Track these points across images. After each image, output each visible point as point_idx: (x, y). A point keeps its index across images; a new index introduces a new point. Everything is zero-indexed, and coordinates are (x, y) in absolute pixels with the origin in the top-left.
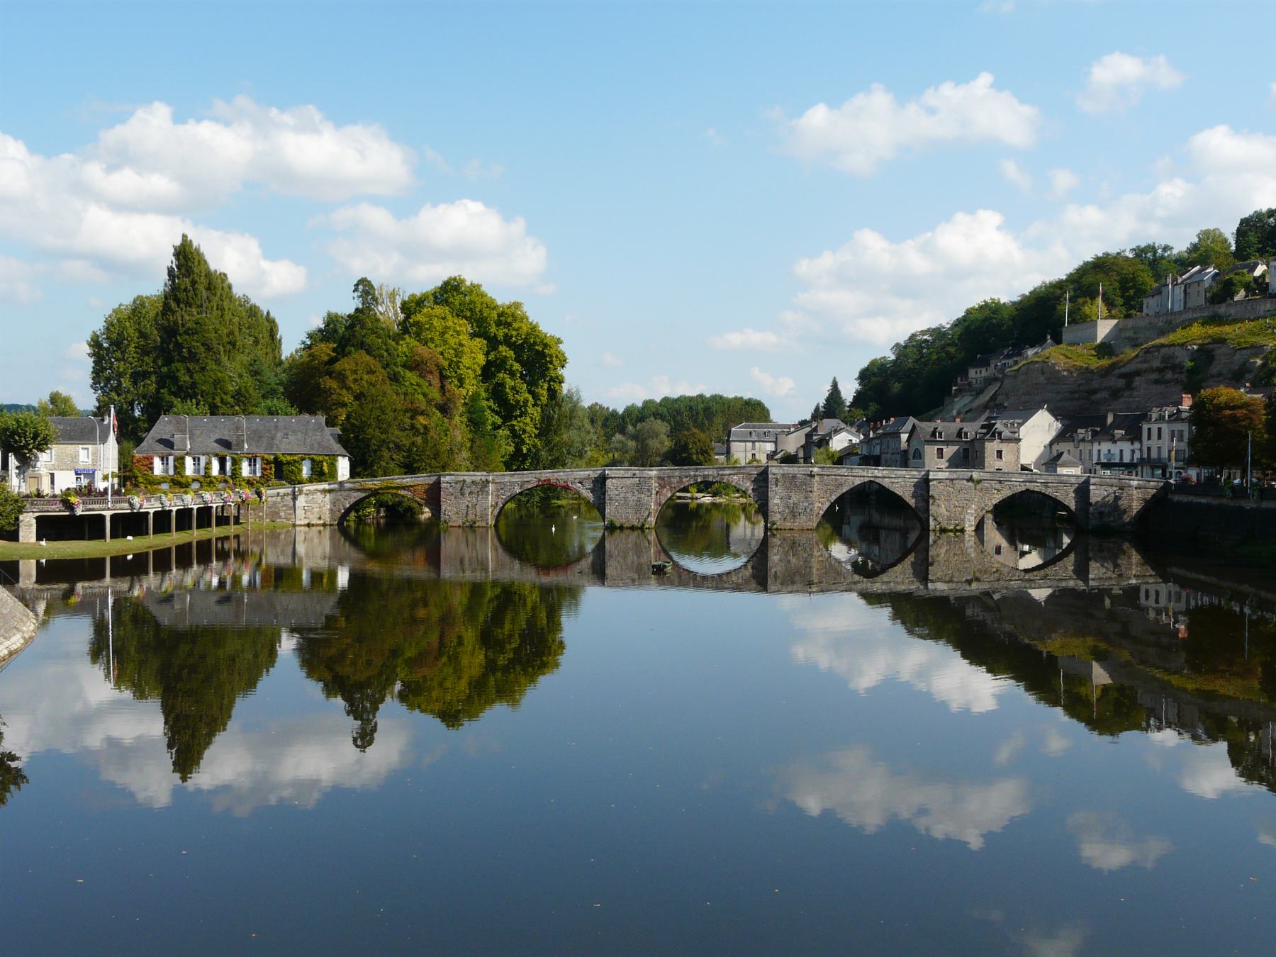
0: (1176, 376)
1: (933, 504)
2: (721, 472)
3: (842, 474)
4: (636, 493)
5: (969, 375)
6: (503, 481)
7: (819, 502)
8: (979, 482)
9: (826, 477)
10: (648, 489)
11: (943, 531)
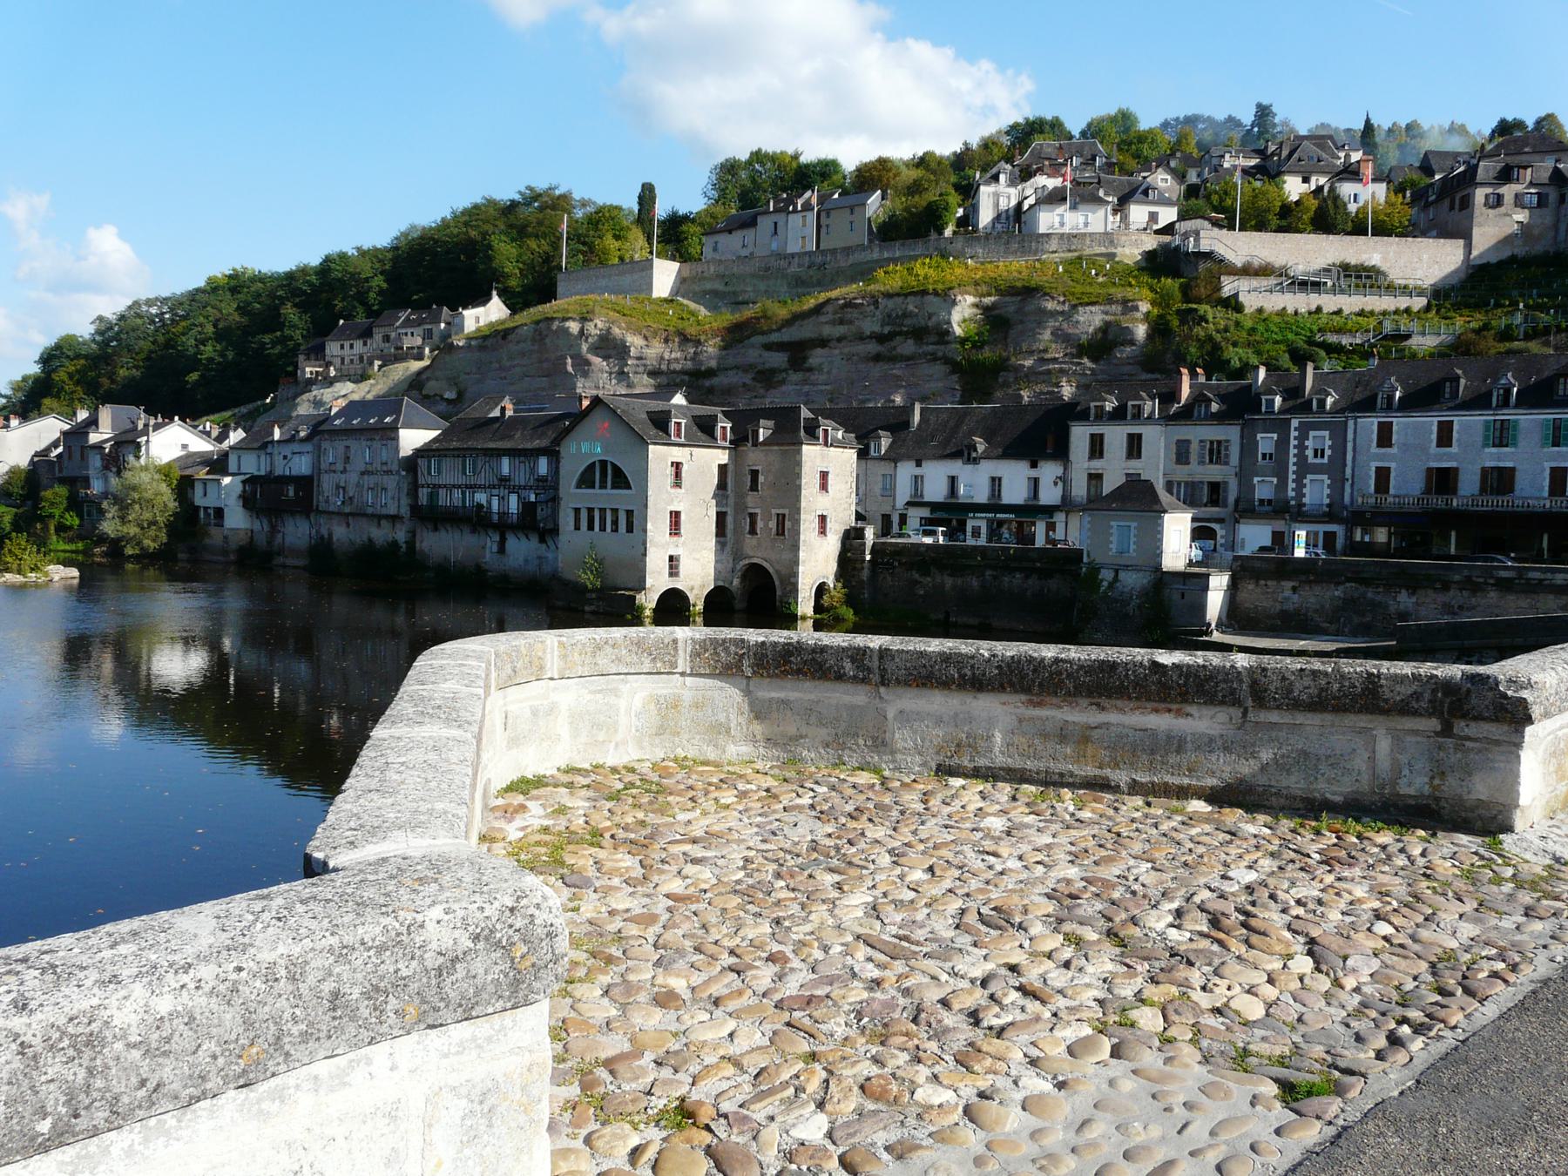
0: (931, 348)
5: (328, 351)
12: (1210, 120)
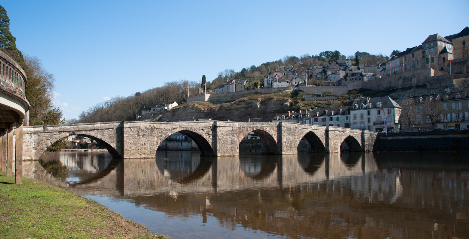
2: (263, 125)
3: (303, 128)
4: (231, 136)
6: (161, 127)
10: (236, 133)
12: (331, 52)
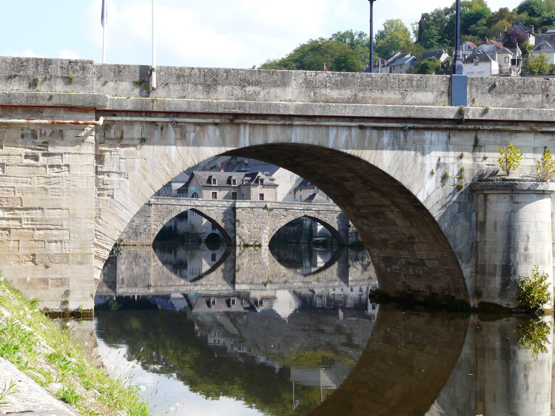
1: (238, 226)
3: (171, 203)
7: (155, 225)
8: (271, 210)
9: (159, 206)
11: (246, 246)
